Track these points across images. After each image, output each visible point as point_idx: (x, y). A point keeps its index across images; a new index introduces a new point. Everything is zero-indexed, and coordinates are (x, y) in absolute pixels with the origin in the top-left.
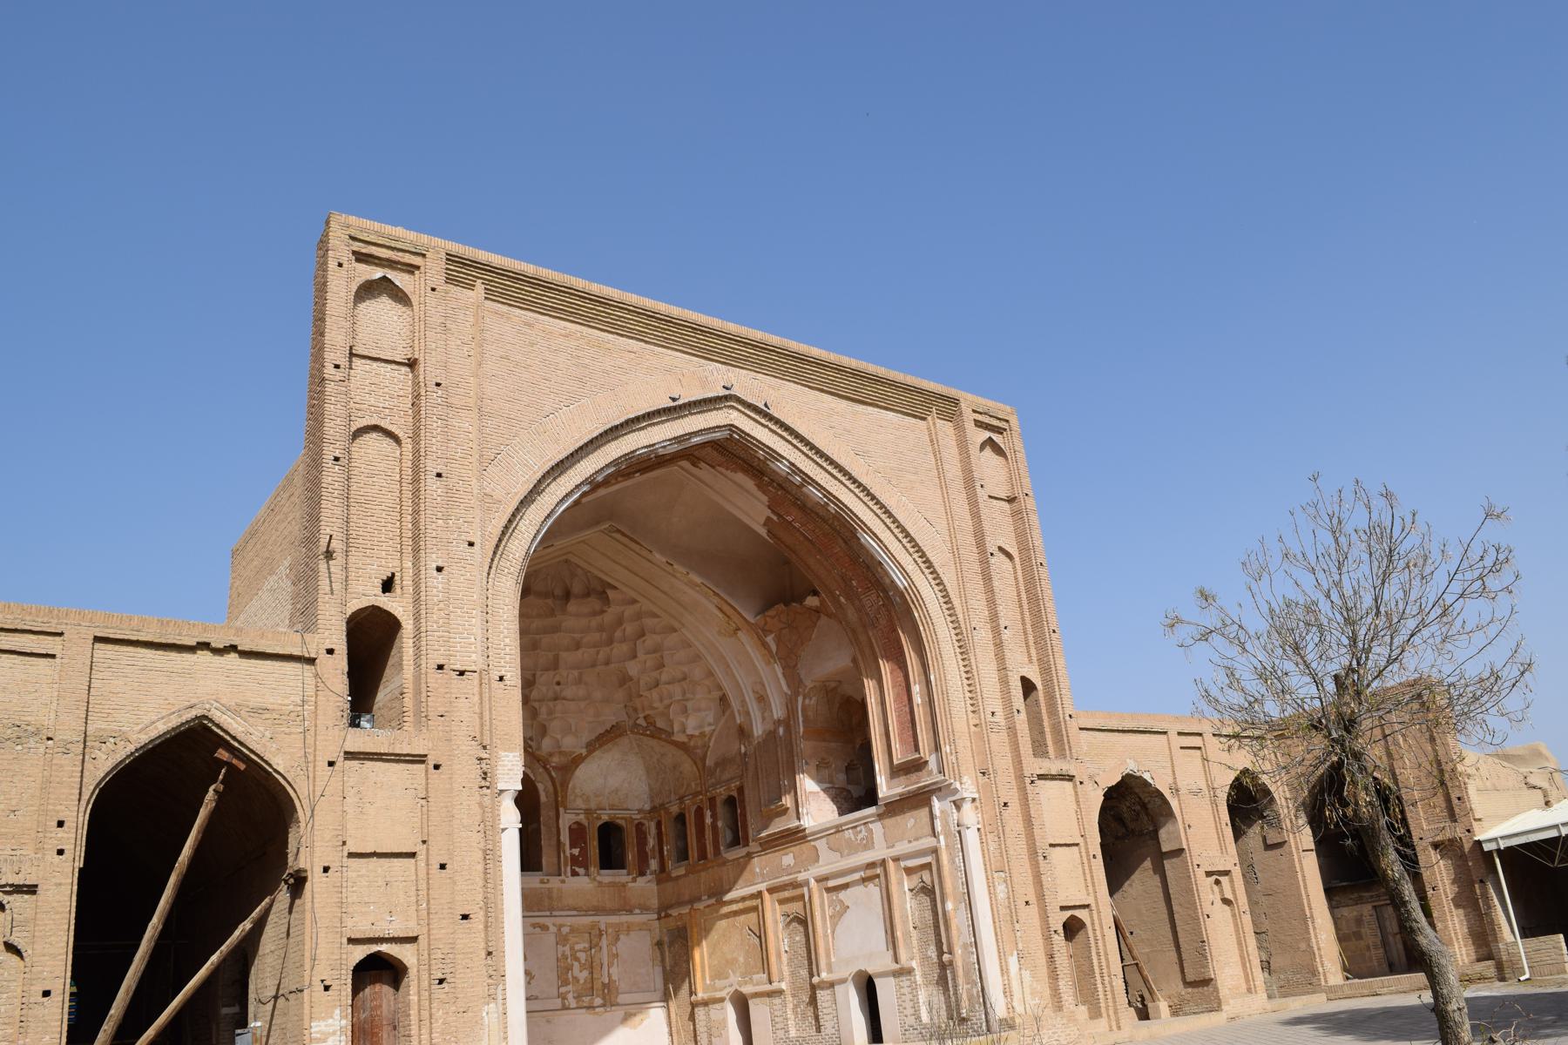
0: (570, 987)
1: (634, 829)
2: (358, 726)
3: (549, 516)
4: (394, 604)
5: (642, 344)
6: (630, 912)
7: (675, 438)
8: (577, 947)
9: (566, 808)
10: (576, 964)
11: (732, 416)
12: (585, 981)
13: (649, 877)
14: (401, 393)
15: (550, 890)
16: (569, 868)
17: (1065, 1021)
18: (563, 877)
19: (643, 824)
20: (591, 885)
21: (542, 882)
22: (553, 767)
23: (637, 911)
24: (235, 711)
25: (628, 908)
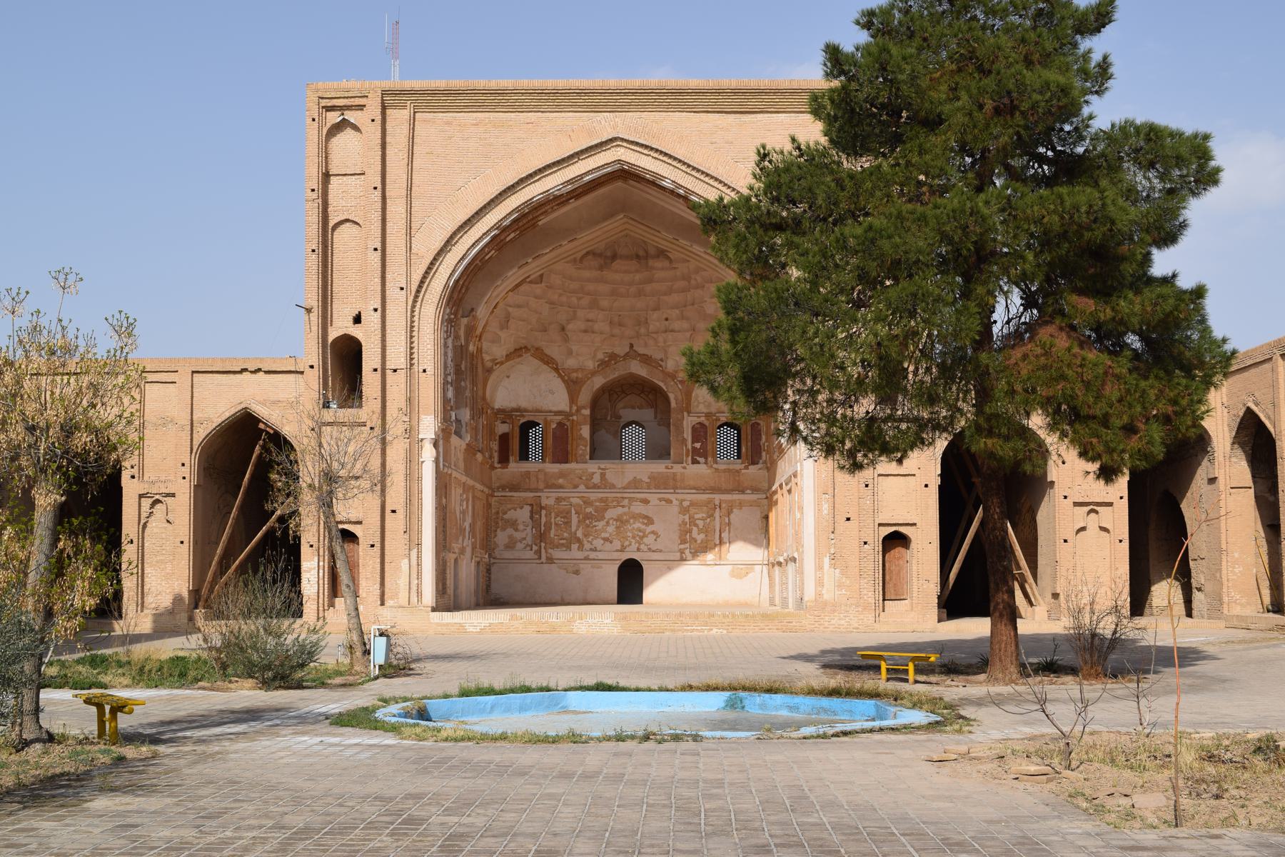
0: (687, 545)
1: (749, 428)
2: (328, 407)
3: (462, 259)
4: (356, 332)
5: (540, 114)
6: (743, 492)
7: (568, 181)
8: (696, 516)
9: (689, 413)
10: (695, 529)
11: (619, 153)
12: (702, 541)
13: (760, 466)
14: (362, 194)
15: (674, 474)
16: (690, 458)
17: (860, 609)
18: (685, 465)
19: (758, 424)
20: (709, 471)
21: (667, 468)
22: (680, 382)
23: (749, 491)
24: (263, 403)
25: (741, 489)
